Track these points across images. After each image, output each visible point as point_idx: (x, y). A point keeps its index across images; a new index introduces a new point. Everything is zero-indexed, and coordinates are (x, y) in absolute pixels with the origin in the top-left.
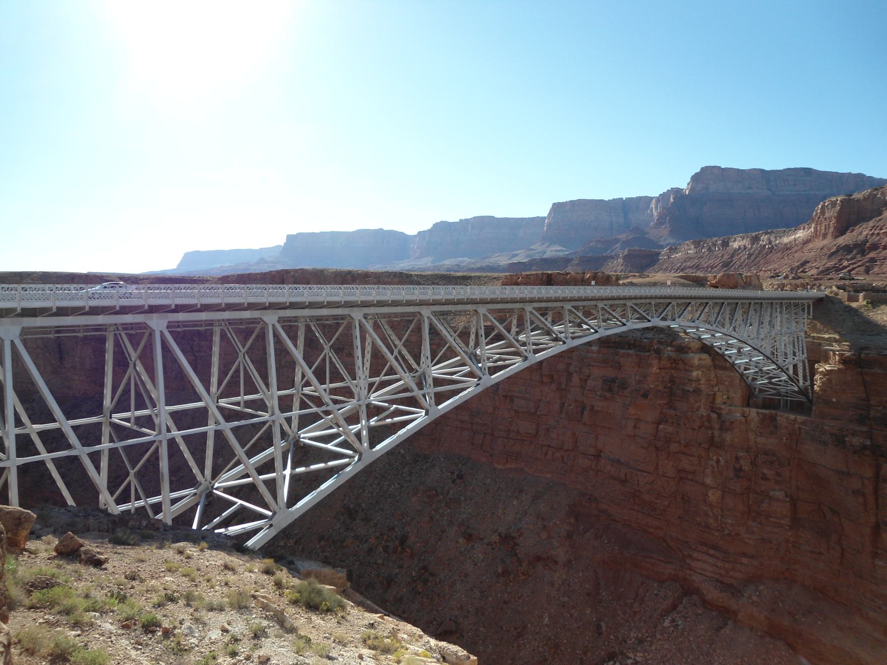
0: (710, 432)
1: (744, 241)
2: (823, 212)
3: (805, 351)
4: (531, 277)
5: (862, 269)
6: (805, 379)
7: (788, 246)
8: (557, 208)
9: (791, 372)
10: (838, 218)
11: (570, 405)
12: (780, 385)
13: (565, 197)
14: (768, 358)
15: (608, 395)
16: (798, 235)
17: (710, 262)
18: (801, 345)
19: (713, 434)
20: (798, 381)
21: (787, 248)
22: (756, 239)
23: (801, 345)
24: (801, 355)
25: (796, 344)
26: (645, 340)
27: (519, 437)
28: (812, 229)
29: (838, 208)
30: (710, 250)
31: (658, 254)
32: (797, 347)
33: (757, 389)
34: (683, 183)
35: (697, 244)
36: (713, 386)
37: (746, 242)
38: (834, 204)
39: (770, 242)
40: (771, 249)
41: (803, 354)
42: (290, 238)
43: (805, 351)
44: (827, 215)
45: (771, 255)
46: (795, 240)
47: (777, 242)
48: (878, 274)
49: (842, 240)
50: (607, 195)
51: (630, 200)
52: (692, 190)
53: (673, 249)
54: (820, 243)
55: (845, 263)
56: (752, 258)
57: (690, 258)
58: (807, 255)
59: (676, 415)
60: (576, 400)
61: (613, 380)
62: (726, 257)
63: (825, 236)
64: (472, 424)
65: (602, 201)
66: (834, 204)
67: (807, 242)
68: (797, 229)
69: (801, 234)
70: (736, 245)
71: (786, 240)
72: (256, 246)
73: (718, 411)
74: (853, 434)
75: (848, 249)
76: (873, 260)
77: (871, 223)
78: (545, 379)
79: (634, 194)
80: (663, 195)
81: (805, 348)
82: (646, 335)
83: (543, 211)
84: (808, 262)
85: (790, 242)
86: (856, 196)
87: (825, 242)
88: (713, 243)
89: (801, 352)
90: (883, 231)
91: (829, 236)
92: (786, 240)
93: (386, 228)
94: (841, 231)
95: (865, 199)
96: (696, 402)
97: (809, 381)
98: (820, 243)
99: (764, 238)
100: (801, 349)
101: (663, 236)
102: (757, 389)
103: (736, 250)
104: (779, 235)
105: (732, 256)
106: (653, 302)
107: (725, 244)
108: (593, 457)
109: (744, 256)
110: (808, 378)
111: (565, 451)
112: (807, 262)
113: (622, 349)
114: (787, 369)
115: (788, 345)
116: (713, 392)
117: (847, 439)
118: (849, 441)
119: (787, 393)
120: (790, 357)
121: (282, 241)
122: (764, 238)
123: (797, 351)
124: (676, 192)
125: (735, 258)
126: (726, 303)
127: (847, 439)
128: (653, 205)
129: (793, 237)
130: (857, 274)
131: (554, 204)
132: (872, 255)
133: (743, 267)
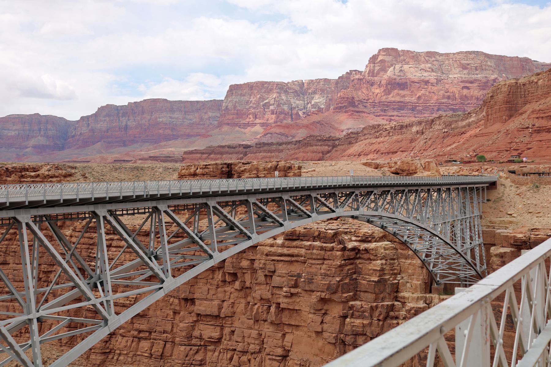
1: (423, 124)
3: (481, 235)
4: (211, 167)
6: (482, 263)
7: (463, 130)
9: (469, 257)
11: (256, 304)
12: (459, 270)
14: (447, 243)
15: (293, 290)
16: (471, 120)
17: (391, 147)
18: (476, 230)
20: (475, 265)
23: (476, 230)
24: (477, 239)
25: (473, 228)
26: (330, 231)
27: (202, 343)
28: (484, 113)
32: (473, 232)
33: (438, 276)
36: (396, 274)
41: (479, 237)
43: (481, 235)
45: (447, 139)
46: (469, 125)
47: (453, 126)
48: (544, 156)
56: (430, 142)
59: (362, 307)
60: (261, 299)
61: (299, 276)
64: (150, 333)
70: (415, 129)
73: (402, 300)
78: (228, 278)
81: (481, 232)
82: (330, 226)
85: (464, 127)
88: (392, 127)
89: (477, 236)
90: (546, 115)
96: (382, 292)
97: (485, 264)
100: (477, 233)
102: (438, 276)
104: (454, 119)
105: (412, 141)
108: (280, 358)
110: (485, 261)
111: (252, 354)
113: (308, 240)
114: (466, 254)
115: (465, 230)
116: (397, 281)
119: (466, 277)
120: (468, 241)
123: (473, 235)
126: (407, 190)
129: (467, 121)
133: (422, 151)
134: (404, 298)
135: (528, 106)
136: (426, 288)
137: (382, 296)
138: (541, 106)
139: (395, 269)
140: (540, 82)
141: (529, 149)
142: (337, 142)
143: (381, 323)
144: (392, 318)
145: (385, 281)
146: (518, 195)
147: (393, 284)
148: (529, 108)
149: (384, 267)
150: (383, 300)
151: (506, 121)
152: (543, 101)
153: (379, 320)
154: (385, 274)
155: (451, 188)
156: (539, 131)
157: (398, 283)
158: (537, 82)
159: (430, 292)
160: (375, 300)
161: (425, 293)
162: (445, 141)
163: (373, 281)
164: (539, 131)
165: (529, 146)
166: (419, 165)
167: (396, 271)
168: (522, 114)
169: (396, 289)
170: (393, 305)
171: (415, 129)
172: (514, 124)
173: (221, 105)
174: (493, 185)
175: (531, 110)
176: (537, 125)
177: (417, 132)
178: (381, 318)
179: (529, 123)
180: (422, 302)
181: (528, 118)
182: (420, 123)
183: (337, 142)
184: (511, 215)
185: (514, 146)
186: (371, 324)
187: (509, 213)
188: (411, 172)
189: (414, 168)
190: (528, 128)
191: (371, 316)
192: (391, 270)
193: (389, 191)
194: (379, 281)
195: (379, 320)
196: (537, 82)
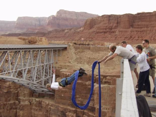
0: (15, 110)
19: (17, 111)
36: (17, 88)
40: (74, 33)
46: (80, 30)
52: (57, 15)
54: (85, 31)
57: (54, 35)
67: (83, 31)
70: (66, 31)
74: (69, 112)
80: (49, 17)
85: (79, 31)
96: (9, 97)
105: (65, 34)
116: (17, 92)
117: (67, 114)
118: (68, 115)
126: (39, 50)
127: (67, 114)
128: (47, 20)
129: (80, 30)
131: (18, 17)
134: (20, 99)
135: (95, 26)
136: (30, 95)
137: (9, 98)
138: (99, 26)
139: (16, 86)
140: (99, 19)
141: (94, 38)
142: (45, 34)
143: (8, 111)
144: (14, 109)
145: (11, 92)
146: (75, 53)
147: (15, 93)
148: (96, 26)
149: (11, 85)
150: (9, 101)
151: (89, 29)
152: (99, 25)
153: (7, 110)
154: (11, 88)
155: (46, 50)
156: (98, 33)
157: (18, 92)
158: (98, 19)
159: (33, 96)
160: (6, 101)
161: (30, 97)
162: (74, 35)
163: (4, 92)
164: (98, 33)
165: (95, 37)
166: (38, 39)
167: (17, 87)
168: (93, 28)
169: (17, 95)
170: (15, 103)
171: (66, 31)
172: (91, 30)
173: (15, 23)
174: (65, 48)
175: (96, 27)
176: (97, 31)
177: (67, 32)
178: (8, 109)
179: (95, 30)
180: (27, 102)
181: (95, 29)
182: (68, 29)
183: (45, 34)
184: (70, 62)
185: (91, 37)
186: (4, 112)
187: (69, 61)
188: (35, 42)
189: (35, 40)
190: (95, 32)
191: (4, 108)
192: (15, 86)
193: (7, 52)
194: (7, 92)
195: (7, 110)
196: (98, 19)
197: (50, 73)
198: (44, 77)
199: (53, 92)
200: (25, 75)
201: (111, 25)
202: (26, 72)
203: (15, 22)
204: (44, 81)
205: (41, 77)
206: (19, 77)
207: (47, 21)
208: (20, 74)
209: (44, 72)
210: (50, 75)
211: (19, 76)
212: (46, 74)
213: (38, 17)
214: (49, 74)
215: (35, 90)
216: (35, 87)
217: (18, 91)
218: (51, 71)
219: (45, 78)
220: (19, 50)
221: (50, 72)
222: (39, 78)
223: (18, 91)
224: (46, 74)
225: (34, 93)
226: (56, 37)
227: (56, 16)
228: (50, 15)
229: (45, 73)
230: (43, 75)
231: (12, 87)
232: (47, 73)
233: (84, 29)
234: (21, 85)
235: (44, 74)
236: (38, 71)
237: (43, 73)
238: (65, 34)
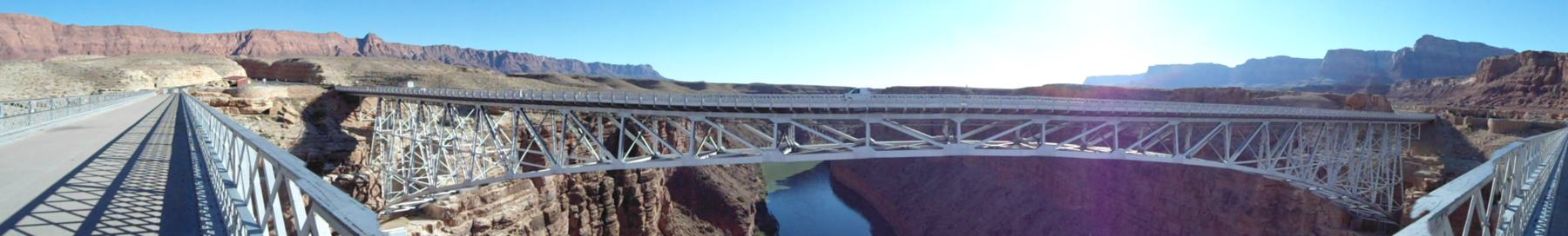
2: (1482, 66)
5: (1500, 103)
8: (1331, 53)
10: (1491, 70)
13: (1335, 47)
21: (1463, 88)
22: (1446, 81)
29: (1490, 64)
30: (1419, 86)
31: (1389, 87)
34: (1411, 44)
35: (1413, 82)
37: (1441, 83)
38: (1488, 61)
39: (1454, 84)
40: (1454, 88)
42: (1151, 68)
44: (1484, 68)
49: (1491, 84)
50: (1366, 49)
51: (1379, 52)
52: (1416, 49)
53: (1398, 85)
54: (1479, 85)
55: (1492, 98)
57: (1407, 91)
58: (1472, 92)
62: (1429, 91)
63: (1482, 81)
65: (1361, 51)
66: (1488, 61)
67: (1473, 85)
68: (1468, 78)
69: (1472, 80)
71: (1463, 83)
72: (1130, 73)
75: (1493, 90)
76: (1510, 97)
77: (1512, 75)
79: (1382, 49)
80: (1399, 51)
83: (1321, 55)
84: (1470, 96)
86: (1501, 58)
87: (1482, 85)
91: (1485, 82)
92: (1463, 83)
93: (1215, 62)
94: (1491, 80)
95: (1510, 60)
98: (1479, 85)
99: (1452, 80)
101: (1396, 75)
103: (1435, 87)
105: (1432, 90)
106: (1386, 123)
107: (1429, 83)
109: (1439, 91)
112: (1470, 96)
121: (1145, 70)
122: (1452, 80)
124: (1407, 50)
125: (1434, 92)
128: (1393, 56)
130: (1497, 106)
132: (1510, 94)
177: (1437, 86)
197: (1391, 177)
198: (1376, 185)
199: (1394, 220)
200: (1332, 175)
201: (1542, 74)
202: (1336, 172)
203: (1320, 60)
204: (1375, 193)
205: (1370, 184)
206: (1321, 180)
207: (1394, 62)
208: (1322, 173)
209: (1378, 174)
210: (1391, 182)
211: (1320, 178)
212: (1382, 179)
213: (1374, 51)
214: (1388, 178)
215: (1355, 213)
216: (1355, 207)
217: (1317, 212)
218: (1394, 172)
219: (1379, 186)
220: (1322, 121)
221: (1391, 174)
222: (1365, 186)
223: (1317, 212)
224: (1382, 179)
225: (1352, 218)
226: (1411, 97)
227: (1414, 50)
228: (1400, 47)
229: (1380, 175)
230: (1375, 180)
231: (1303, 201)
232: (1385, 176)
233: (1477, 81)
234: (1324, 198)
235: (1378, 177)
236: (1365, 170)
237: (1375, 175)
238: (1432, 90)
